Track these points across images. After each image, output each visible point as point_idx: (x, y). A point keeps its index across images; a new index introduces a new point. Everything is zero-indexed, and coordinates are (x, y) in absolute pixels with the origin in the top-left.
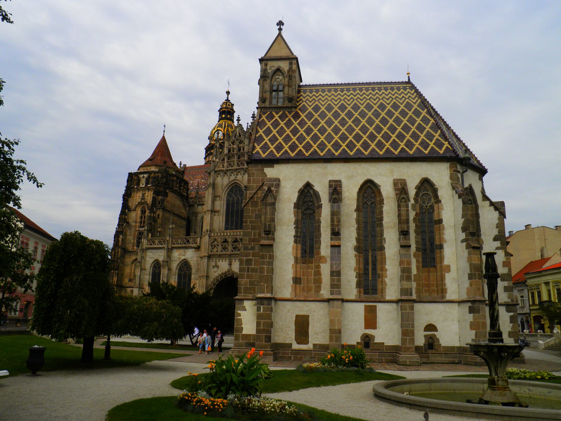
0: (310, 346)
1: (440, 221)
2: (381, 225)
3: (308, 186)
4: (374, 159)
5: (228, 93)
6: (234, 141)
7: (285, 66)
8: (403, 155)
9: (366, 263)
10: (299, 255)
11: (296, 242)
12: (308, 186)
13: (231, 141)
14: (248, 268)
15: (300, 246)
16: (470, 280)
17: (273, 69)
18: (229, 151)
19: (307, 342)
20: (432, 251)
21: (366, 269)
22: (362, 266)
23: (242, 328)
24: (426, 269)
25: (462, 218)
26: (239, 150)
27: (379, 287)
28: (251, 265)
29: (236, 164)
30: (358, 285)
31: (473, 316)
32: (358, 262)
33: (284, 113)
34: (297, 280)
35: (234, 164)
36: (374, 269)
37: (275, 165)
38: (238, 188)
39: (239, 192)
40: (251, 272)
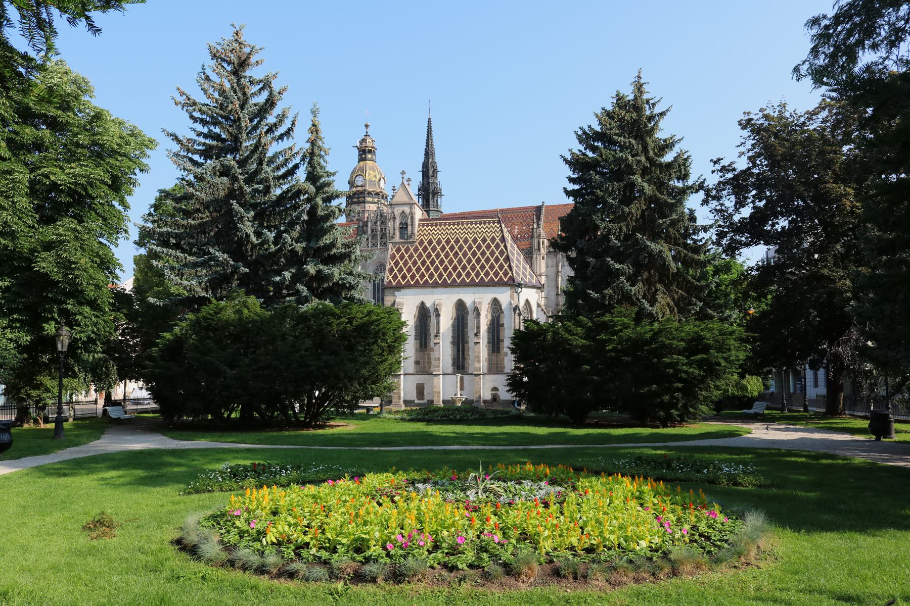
0: (425, 401)
1: (503, 325)
2: (467, 328)
3: (423, 303)
4: (464, 284)
5: (367, 126)
7: (407, 209)
8: (482, 282)
9: (458, 351)
10: (418, 347)
11: (415, 339)
12: (423, 303)
15: (418, 341)
18: (372, 231)
19: (423, 399)
20: (498, 343)
21: (458, 355)
22: (456, 353)
24: (495, 354)
27: (466, 365)
30: (453, 364)
32: (453, 351)
33: (408, 247)
34: (417, 363)
36: (463, 354)
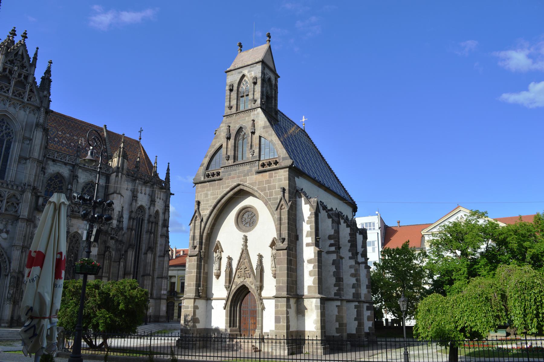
6: (13, 60)
13: (8, 59)
14: (291, 267)
16: (367, 289)
17: (267, 76)
23: (290, 325)
25: (362, 248)
26: (20, 75)
28: (292, 266)
29: (11, 91)
31: (371, 312)
35: (8, 90)
37: (300, 177)
38: (4, 123)
39: (6, 130)
40: (292, 272)
